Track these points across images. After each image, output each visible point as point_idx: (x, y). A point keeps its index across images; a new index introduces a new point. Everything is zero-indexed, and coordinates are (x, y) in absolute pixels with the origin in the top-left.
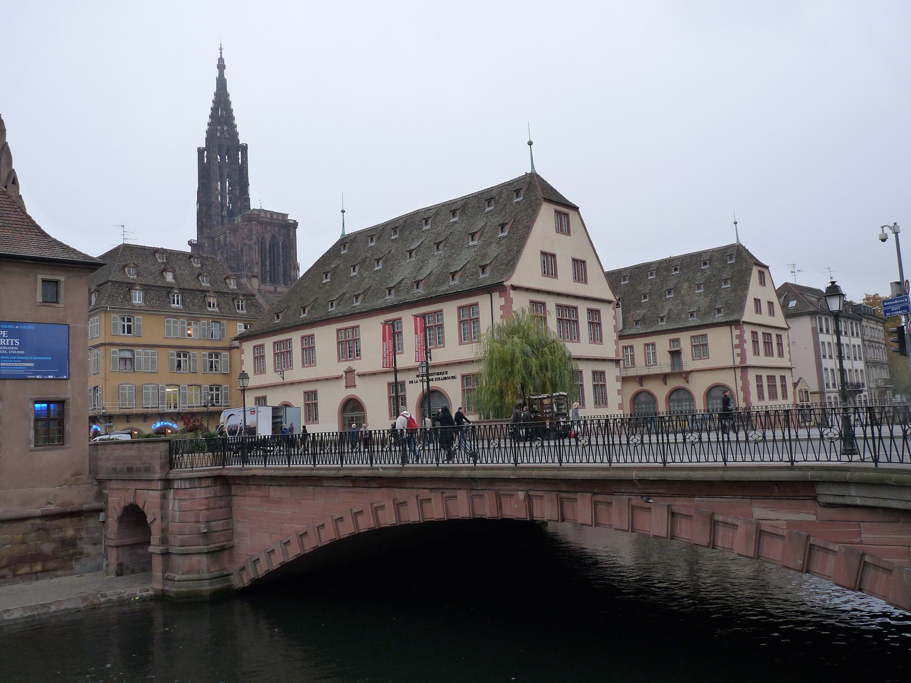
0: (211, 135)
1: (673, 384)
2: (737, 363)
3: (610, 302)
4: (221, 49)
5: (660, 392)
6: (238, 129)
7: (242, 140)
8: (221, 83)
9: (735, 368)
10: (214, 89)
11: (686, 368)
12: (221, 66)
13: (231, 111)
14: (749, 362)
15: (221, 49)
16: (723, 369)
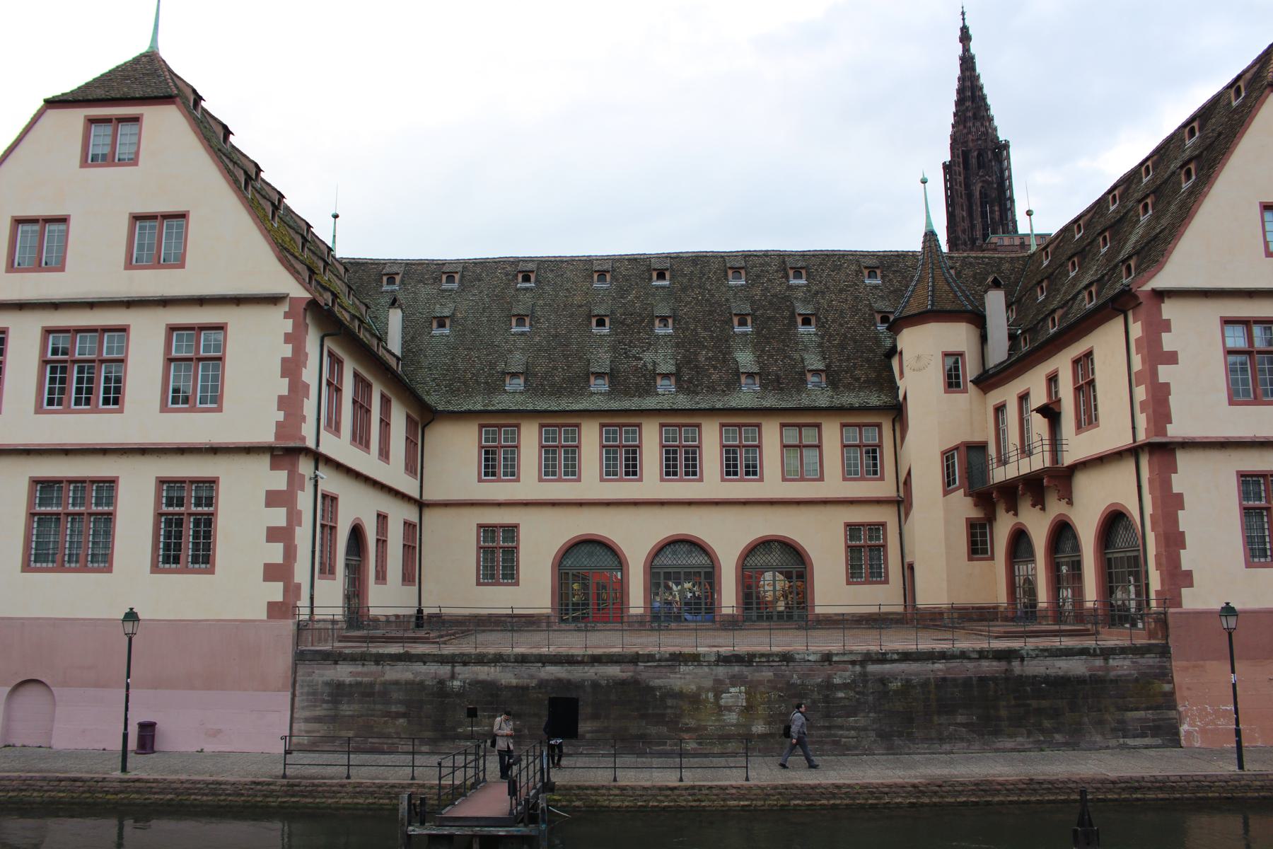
0: (957, 142)
1: (1056, 508)
2: (1142, 437)
3: (274, 300)
4: (963, 14)
5: (1038, 526)
6: (996, 122)
7: (1002, 136)
8: (967, 62)
9: (1134, 452)
10: (958, 72)
11: (1068, 459)
12: (965, 37)
13: (983, 98)
14: (1175, 431)
15: (963, 14)
16: (1117, 456)
